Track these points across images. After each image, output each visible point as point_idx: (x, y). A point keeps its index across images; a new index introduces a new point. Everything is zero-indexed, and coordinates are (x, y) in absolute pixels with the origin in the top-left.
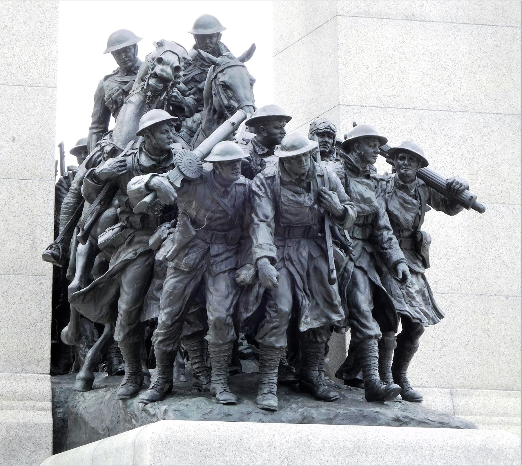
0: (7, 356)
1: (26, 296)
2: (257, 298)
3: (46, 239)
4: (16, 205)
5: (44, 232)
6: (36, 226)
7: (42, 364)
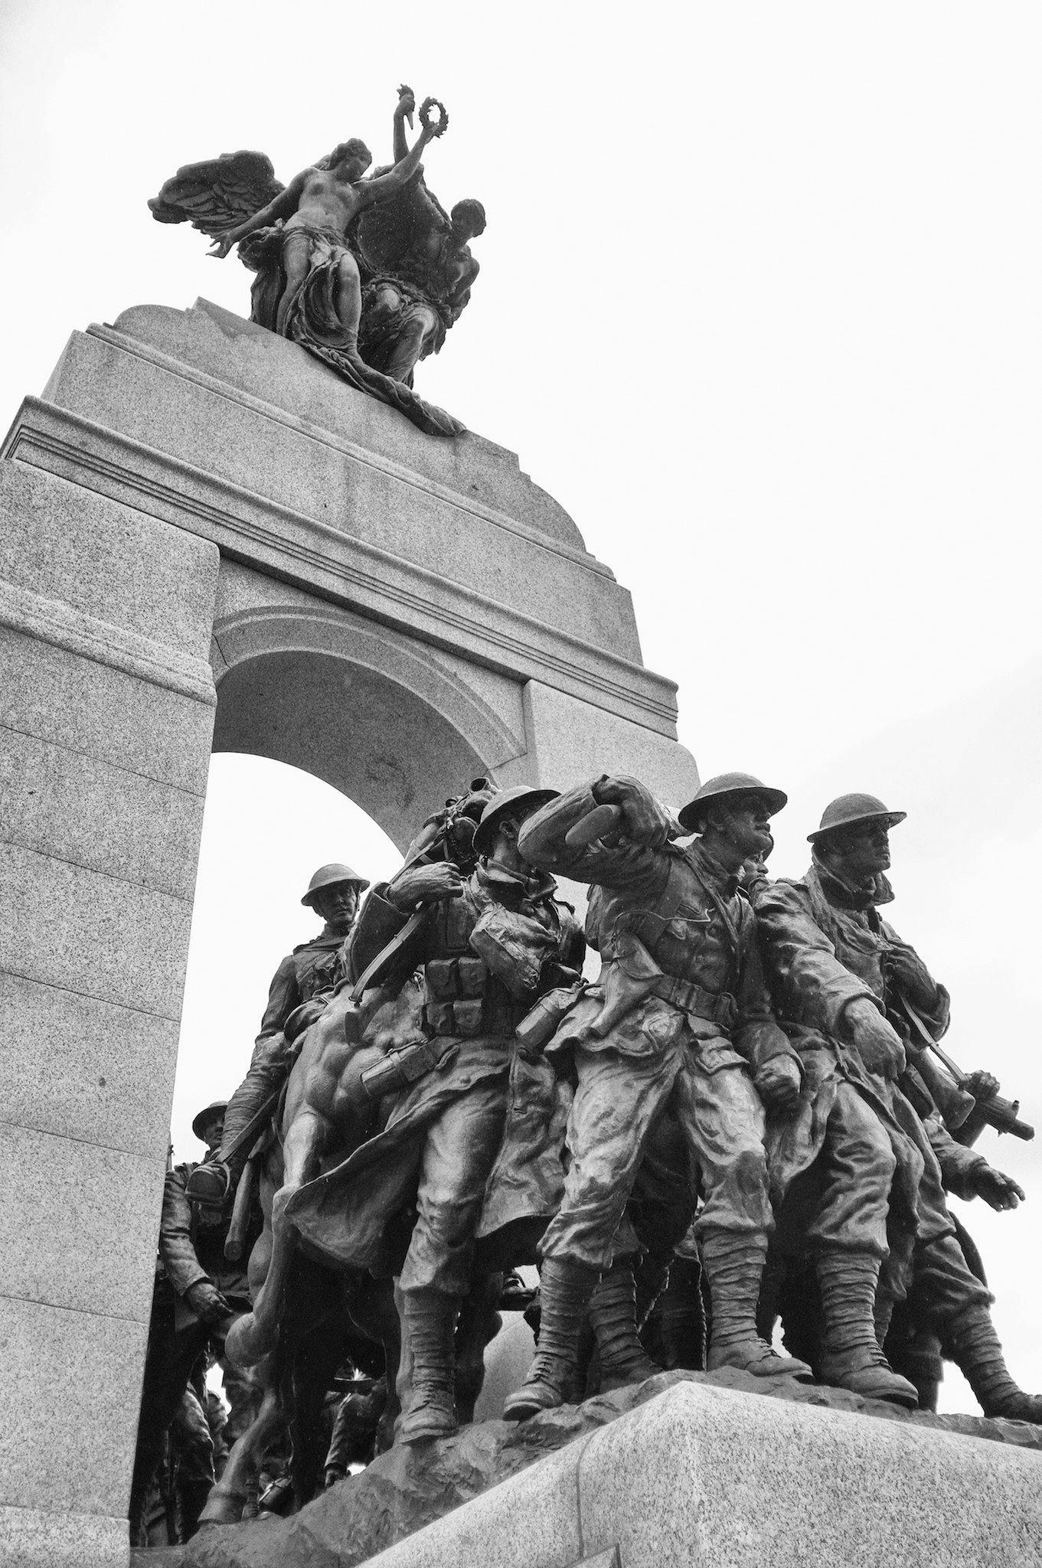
0: (44, 1472)
1: (97, 1354)
2: (814, 1132)
3: (144, 1256)
4: (95, 1188)
5: (141, 1243)
6: (127, 1230)
7: (114, 1496)
